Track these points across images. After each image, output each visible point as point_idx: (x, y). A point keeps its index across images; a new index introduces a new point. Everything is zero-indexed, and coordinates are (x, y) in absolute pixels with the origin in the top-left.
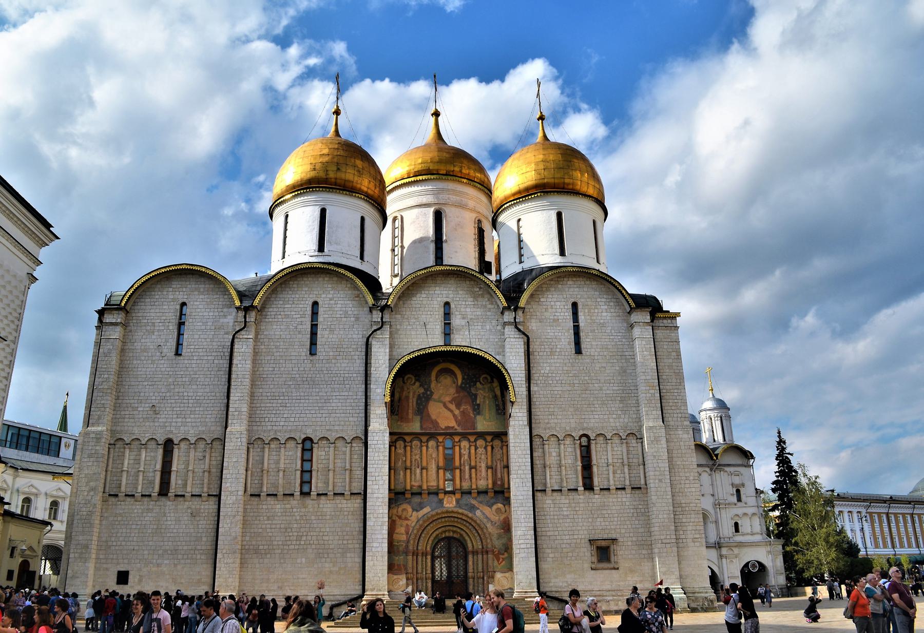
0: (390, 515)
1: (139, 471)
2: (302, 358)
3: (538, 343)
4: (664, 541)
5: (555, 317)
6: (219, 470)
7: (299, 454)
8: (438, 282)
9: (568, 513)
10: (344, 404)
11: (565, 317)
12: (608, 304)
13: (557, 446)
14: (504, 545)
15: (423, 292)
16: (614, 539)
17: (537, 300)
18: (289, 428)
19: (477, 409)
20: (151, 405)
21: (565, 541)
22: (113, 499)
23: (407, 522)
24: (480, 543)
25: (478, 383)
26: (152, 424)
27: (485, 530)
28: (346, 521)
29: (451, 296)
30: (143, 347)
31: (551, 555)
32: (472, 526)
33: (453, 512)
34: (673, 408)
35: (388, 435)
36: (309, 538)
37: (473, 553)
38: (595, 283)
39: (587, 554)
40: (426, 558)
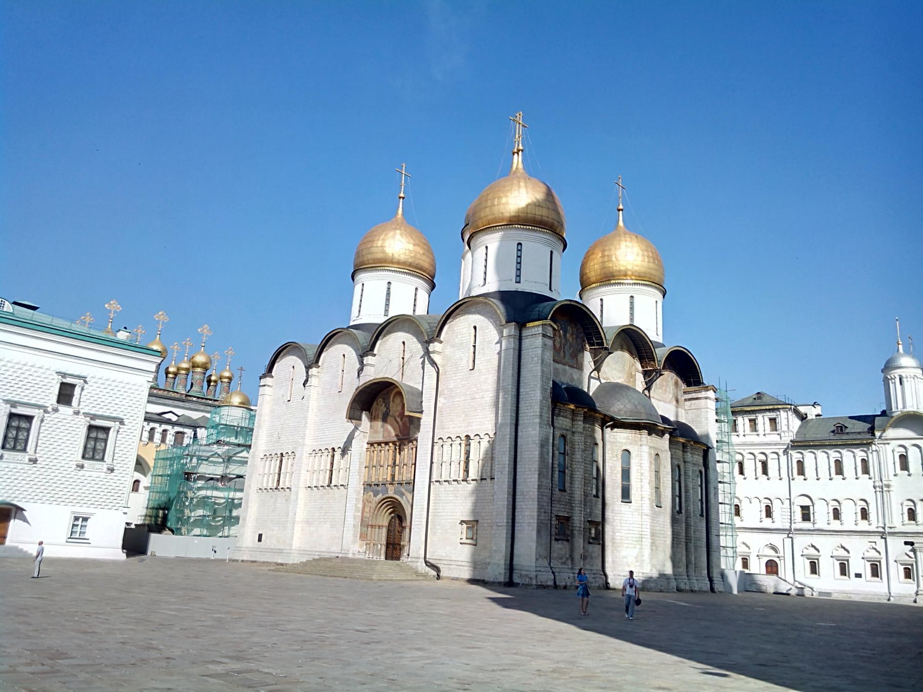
21: (448, 521)
23: (370, 504)
31: (440, 531)
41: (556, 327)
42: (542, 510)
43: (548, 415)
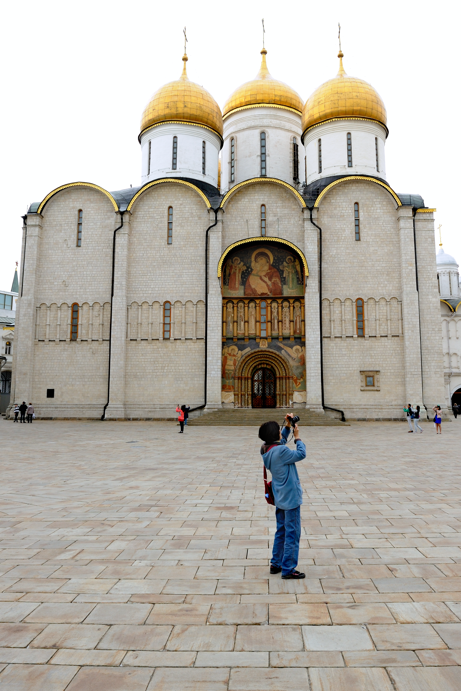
0: (223, 353)
1: (57, 325)
2: (162, 247)
3: (328, 233)
5: (342, 214)
6: (109, 324)
7: (162, 313)
8: (257, 190)
9: (346, 352)
10: (191, 278)
11: (349, 214)
12: (381, 203)
13: (340, 306)
14: (300, 373)
15: (246, 198)
16: (378, 371)
17: (329, 201)
18: (155, 295)
19: (284, 281)
20: (62, 281)
21: (343, 372)
22: (41, 343)
23: (234, 357)
24: (284, 372)
25: (285, 263)
26: (64, 294)
27: (287, 364)
28: (194, 357)
29: (266, 200)
30: (55, 241)
32: (279, 360)
33: (265, 351)
34: (426, 279)
35: (221, 299)
36: (169, 368)
37: (280, 378)
38: (373, 187)
39: (358, 381)
40: (248, 382)
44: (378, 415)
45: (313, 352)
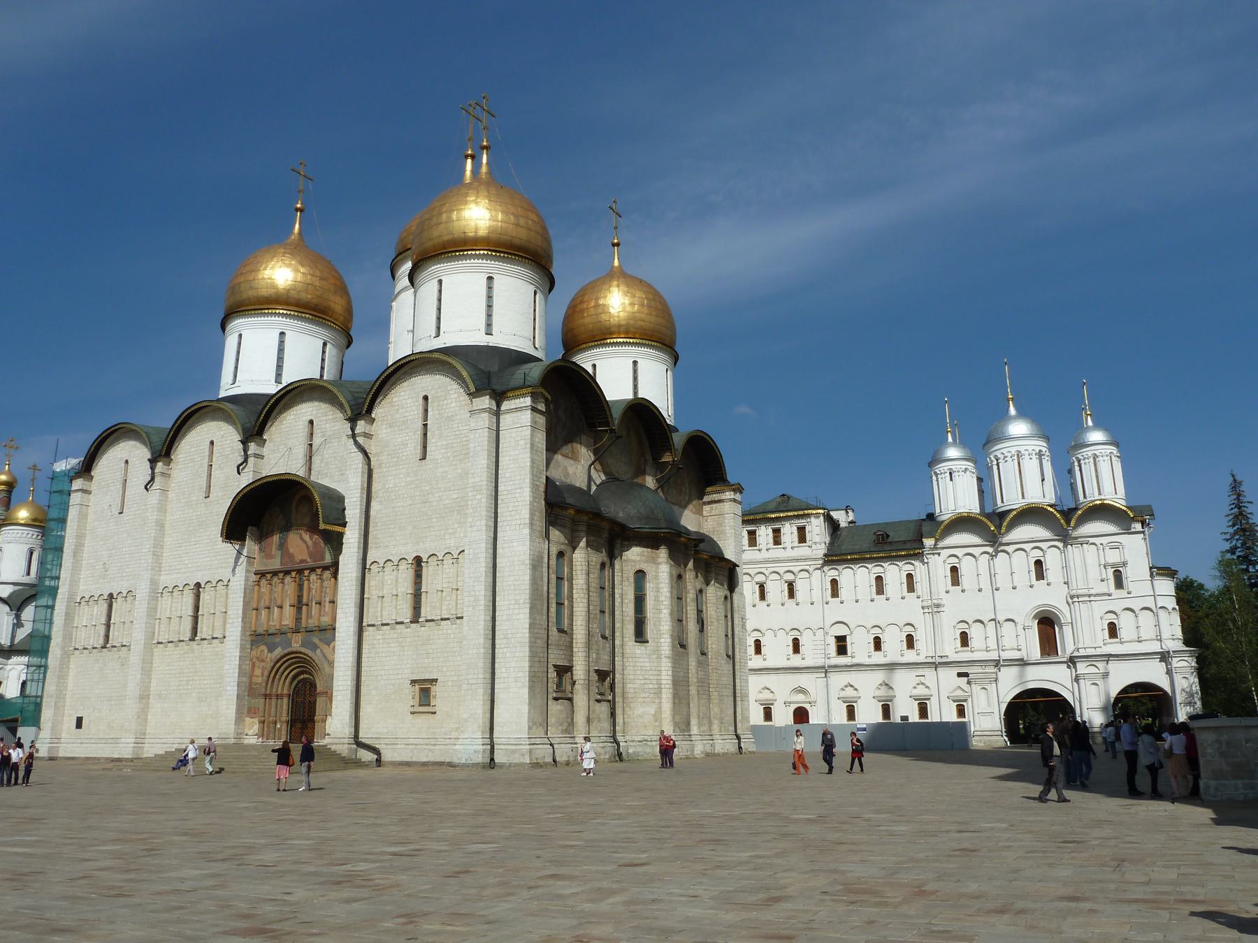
4: (471, 682)
17: (390, 401)
23: (262, 663)
39: (410, 695)
41: (549, 397)
42: (536, 659)
43: (540, 524)
44: (427, 756)
45: (344, 651)
